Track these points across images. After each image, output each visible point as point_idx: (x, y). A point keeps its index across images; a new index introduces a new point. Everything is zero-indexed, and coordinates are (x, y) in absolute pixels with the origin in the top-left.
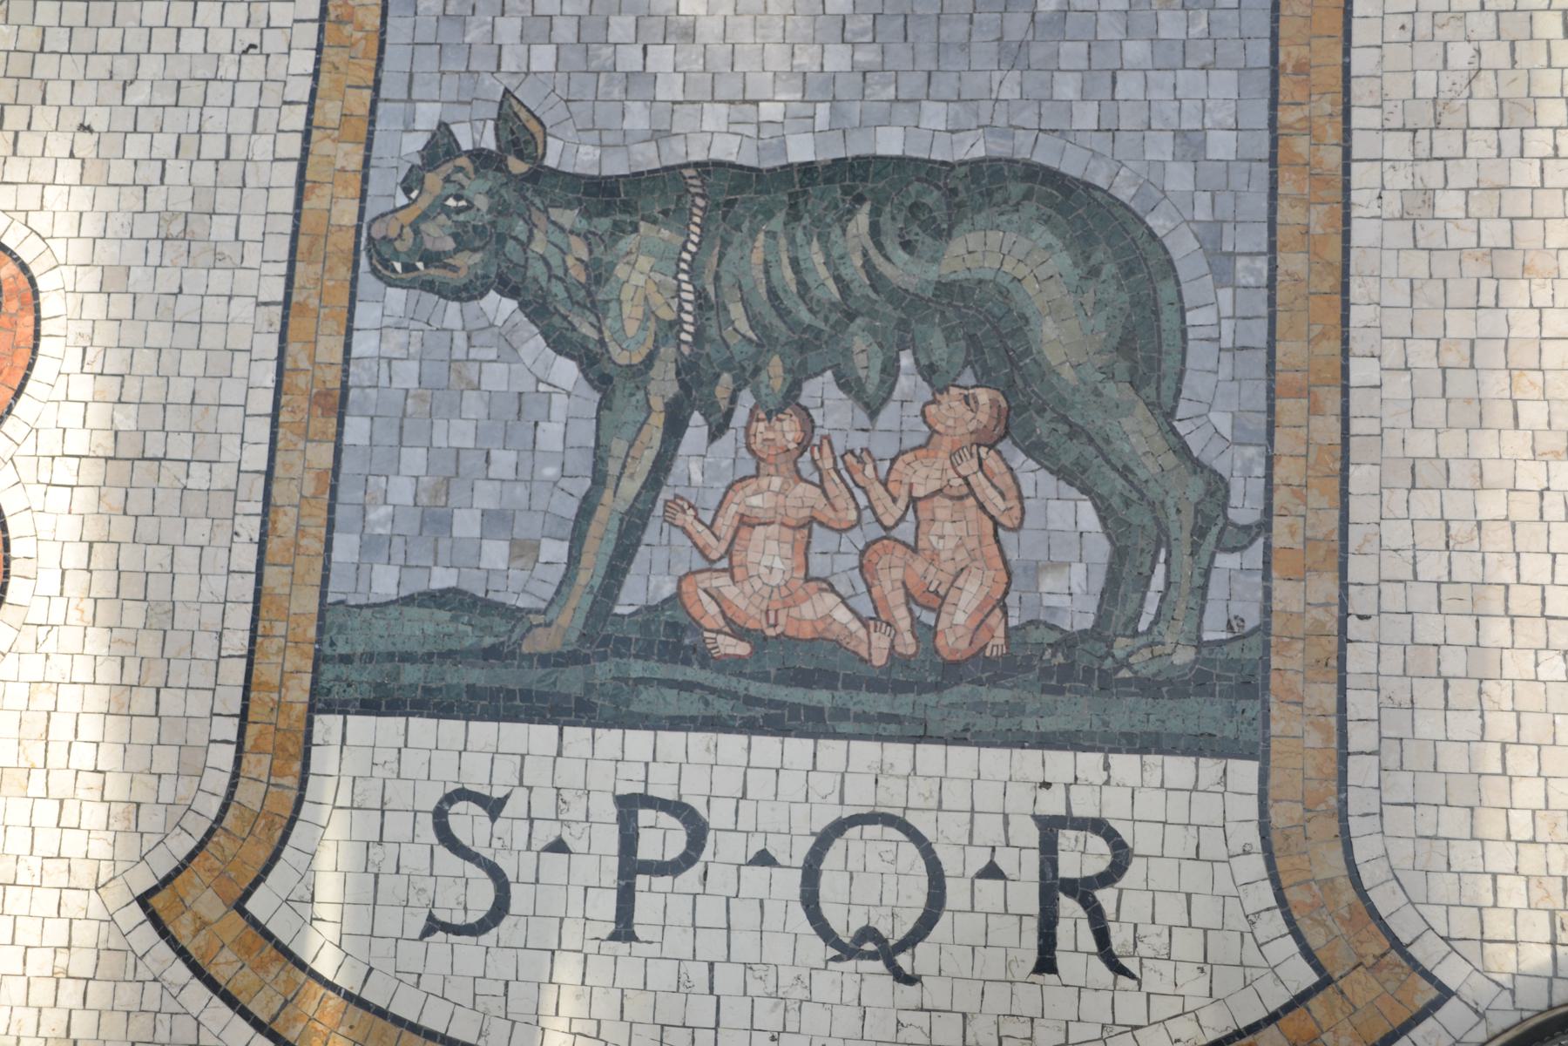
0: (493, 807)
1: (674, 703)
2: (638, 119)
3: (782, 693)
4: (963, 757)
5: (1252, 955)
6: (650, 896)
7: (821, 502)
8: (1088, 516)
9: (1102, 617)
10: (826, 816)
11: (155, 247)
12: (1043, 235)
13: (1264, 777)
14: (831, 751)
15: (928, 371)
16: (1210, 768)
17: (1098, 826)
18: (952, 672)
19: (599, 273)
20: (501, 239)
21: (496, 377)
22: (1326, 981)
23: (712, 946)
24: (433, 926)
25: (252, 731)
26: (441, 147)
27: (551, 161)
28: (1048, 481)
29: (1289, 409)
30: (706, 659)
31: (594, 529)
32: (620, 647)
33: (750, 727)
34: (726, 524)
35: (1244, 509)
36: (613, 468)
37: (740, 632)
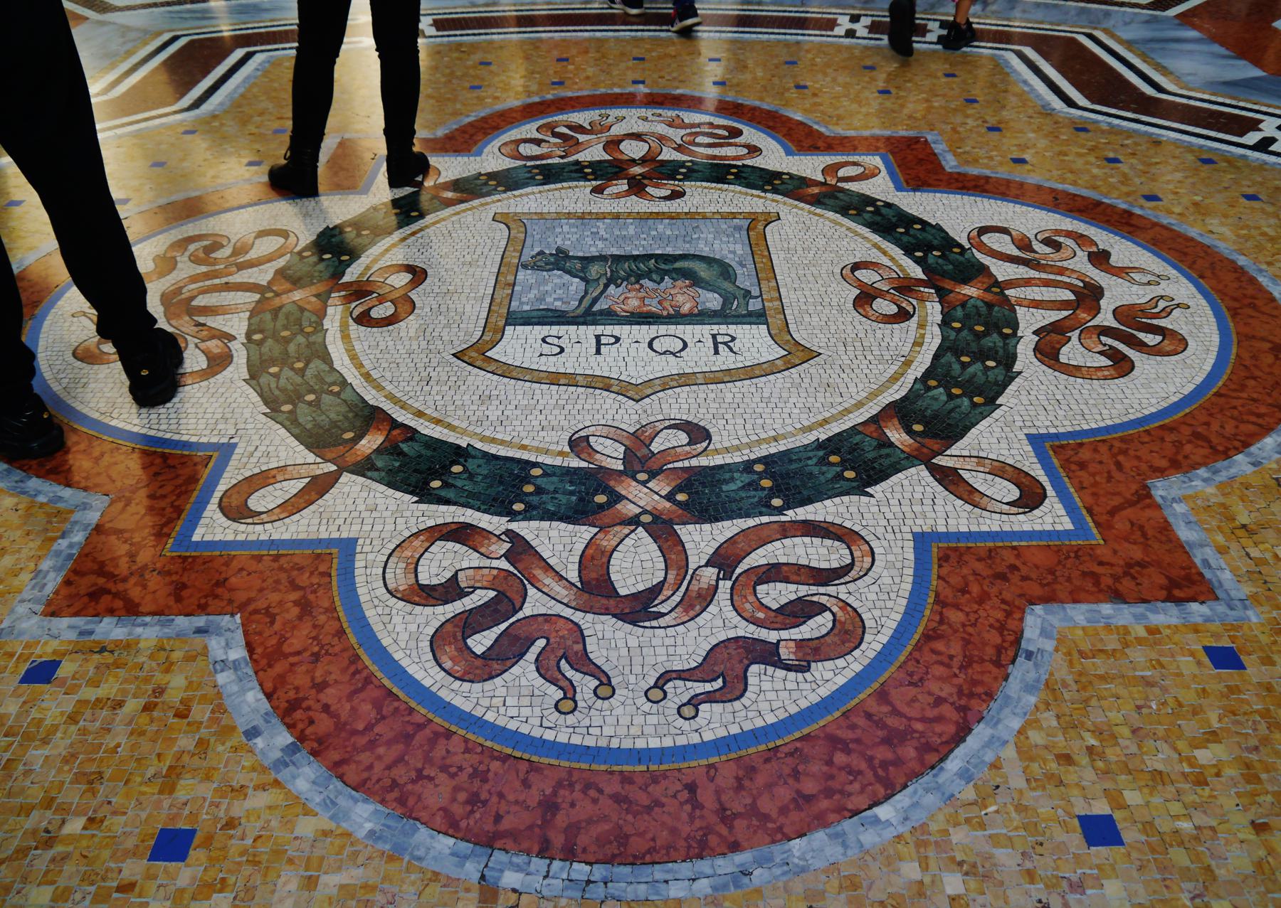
4: (690, 327)
8: (716, 295)
16: (754, 327)
18: (685, 315)
21: (557, 281)
26: (541, 253)
35: (755, 292)
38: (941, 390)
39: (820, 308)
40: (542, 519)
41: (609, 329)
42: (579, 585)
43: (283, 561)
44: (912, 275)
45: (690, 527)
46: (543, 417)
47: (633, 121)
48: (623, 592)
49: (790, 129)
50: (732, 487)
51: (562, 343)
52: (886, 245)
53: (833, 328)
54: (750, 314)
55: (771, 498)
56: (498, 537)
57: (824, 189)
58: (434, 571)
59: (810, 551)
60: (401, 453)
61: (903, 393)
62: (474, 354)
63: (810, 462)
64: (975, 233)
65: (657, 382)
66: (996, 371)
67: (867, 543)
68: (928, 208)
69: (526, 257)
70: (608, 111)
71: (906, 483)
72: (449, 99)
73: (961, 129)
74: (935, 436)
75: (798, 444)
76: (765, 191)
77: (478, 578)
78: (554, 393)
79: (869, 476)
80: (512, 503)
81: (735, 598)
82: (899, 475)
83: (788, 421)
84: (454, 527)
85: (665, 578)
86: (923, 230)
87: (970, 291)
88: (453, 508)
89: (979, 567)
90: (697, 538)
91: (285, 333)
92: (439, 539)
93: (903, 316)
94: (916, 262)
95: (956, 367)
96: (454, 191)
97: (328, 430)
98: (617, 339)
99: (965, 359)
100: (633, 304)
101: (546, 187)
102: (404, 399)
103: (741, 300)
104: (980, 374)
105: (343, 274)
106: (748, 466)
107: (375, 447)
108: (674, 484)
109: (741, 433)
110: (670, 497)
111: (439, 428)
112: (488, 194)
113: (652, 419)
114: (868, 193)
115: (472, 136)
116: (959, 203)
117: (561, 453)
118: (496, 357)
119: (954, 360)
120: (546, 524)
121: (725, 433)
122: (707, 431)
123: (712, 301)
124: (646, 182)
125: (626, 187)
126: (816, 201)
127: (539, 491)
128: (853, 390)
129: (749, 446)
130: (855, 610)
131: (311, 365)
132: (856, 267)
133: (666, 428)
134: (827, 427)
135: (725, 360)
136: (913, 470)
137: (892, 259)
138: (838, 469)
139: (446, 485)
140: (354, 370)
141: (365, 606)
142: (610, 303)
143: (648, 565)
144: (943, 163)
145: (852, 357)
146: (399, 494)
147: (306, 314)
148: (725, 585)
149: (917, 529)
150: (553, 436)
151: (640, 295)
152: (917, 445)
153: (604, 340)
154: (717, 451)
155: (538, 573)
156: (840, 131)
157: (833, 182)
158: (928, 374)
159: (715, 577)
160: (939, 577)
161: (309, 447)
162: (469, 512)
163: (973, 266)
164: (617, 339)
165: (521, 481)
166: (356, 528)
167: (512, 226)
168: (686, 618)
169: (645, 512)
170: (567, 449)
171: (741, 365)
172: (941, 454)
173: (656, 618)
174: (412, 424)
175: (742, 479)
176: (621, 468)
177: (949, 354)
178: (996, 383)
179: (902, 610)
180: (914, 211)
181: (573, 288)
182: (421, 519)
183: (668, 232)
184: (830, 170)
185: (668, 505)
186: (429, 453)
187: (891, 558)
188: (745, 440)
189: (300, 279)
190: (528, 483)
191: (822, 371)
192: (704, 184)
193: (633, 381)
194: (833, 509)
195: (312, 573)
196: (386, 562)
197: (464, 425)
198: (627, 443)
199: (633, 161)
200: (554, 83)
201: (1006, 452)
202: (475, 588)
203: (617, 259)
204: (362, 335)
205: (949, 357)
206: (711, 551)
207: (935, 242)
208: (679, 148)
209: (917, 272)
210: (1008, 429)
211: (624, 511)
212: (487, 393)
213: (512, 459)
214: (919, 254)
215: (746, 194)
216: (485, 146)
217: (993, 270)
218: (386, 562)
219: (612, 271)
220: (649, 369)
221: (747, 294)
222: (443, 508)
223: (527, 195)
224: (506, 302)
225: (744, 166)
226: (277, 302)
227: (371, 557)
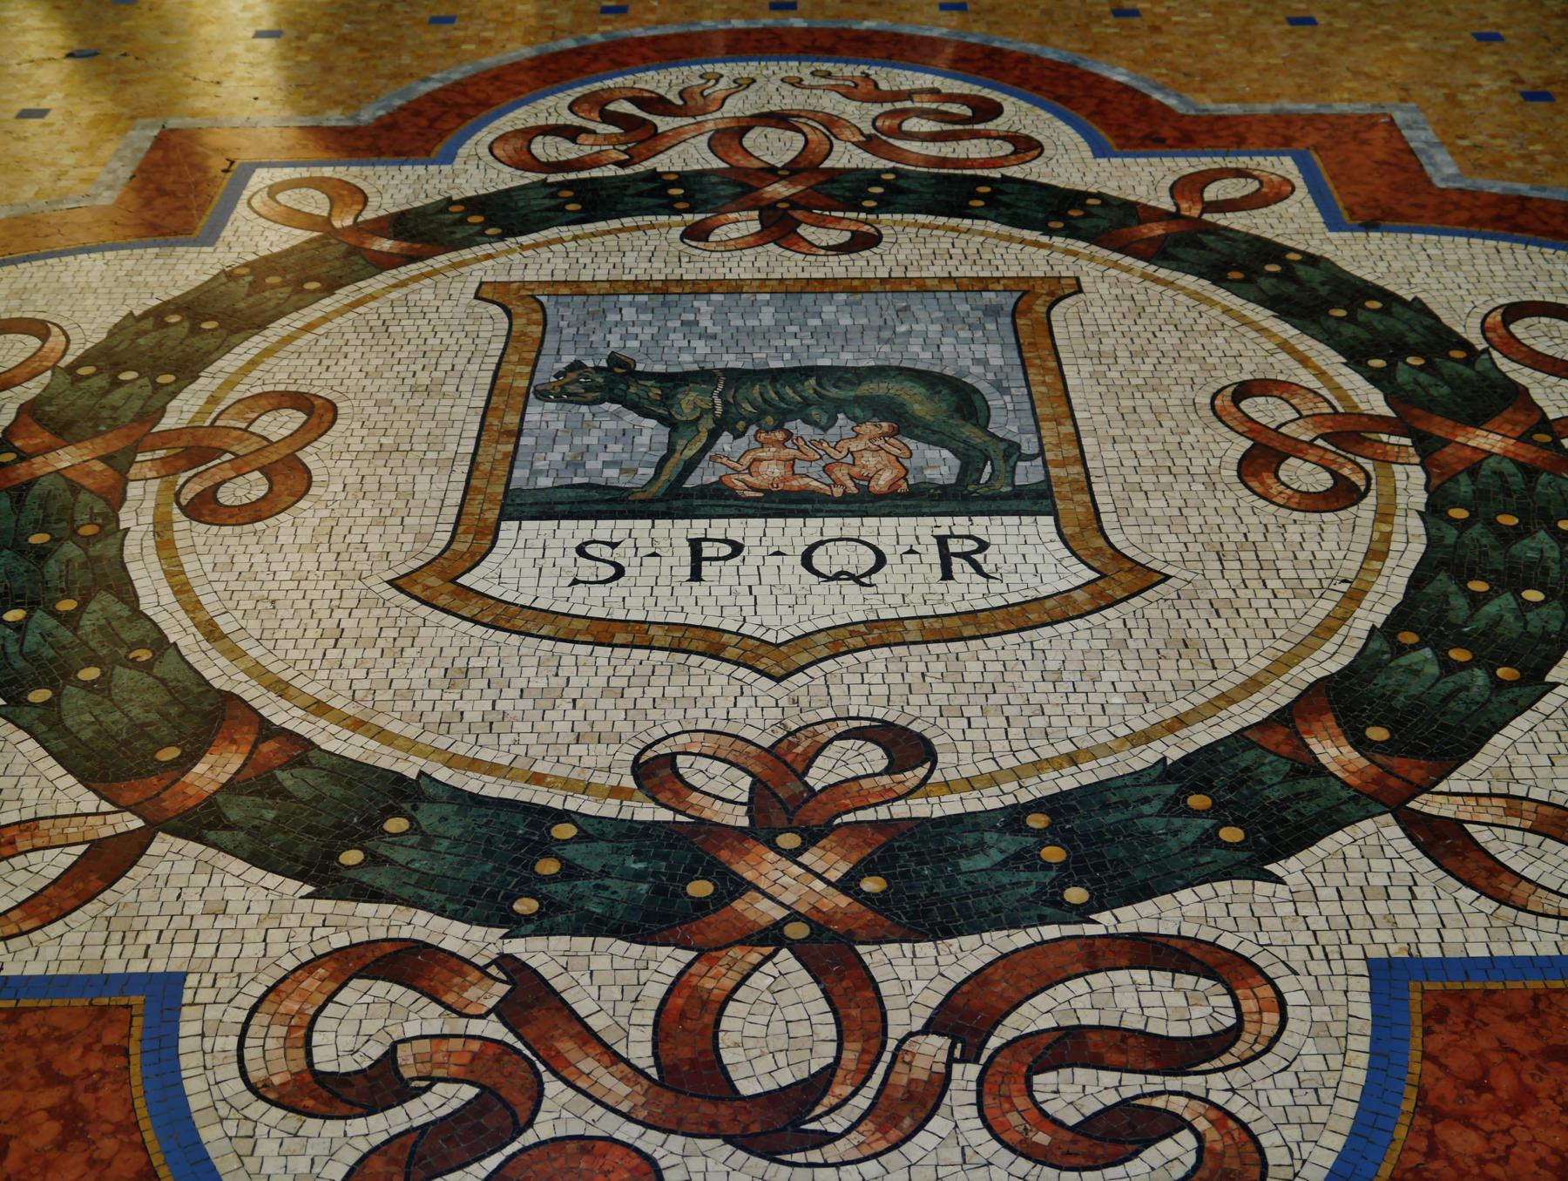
0: (614, 545)
1: (720, 510)
6: (707, 569)
7: (798, 454)
8: (946, 453)
10: (818, 538)
11: (408, 395)
14: (817, 522)
15: (854, 419)
16: (1026, 520)
18: (880, 497)
20: (611, 390)
21: (610, 425)
22: (1103, 576)
24: (575, 582)
25: (461, 529)
26: (576, 366)
27: (639, 367)
28: (922, 446)
30: (737, 498)
31: (669, 465)
33: (766, 516)
34: (746, 461)
35: (1029, 445)
36: (679, 448)
38: (1427, 652)
40: (576, 932)
41: (718, 528)
42: (653, 1072)
43: (26, 1021)
44: (1364, 407)
45: (892, 949)
46: (578, 714)
47: (771, 88)
48: (747, 1088)
49: (1103, 101)
50: (981, 862)
51: (623, 555)
52: (1306, 344)
53: (1195, 522)
54: (1019, 493)
55: (1064, 886)
56: (483, 970)
57: (1174, 227)
58: (346, 1042)
59: (1147, 999)
60: (281, 793)
61: (1344, 659)
62: (433, 581)
63: (1146, 809)
64: (1497, 317)
65: (822, 639)
66: (1544, 610)
67: (1270, 981)
68: (1396, 266)
69: (544, 376)
70: (719, 68)
71: (1352, 852)
72: (385, 45)
73: (1467, 98)
74: (1415, 752)
76: (1050, 233)
77: (439, 1058)
78: (602, 662)
79: (1273, 838)
80: (512, 898)
81: (988, 1100)
82: (1339, 835)
83: (1100, 721)
84: (388, 948)
85: (838, 1059)
86: (1385, 311)
87: (1487, 440)
88: (386, 909)
89: (1513, 1033)
90: (906, 972)
91: (38, 539)
92: (359, 975)
93: (1343, 495)
94: (1371, 380)
95: (1459, 603)
96: (395, 236)
97: (126, 743)
98: (737, 548)
99: (1478, 586)
100: (771, 472)
101: (589, 227)
102: (286, 676)
103: (1000, 463)
104: (1509, 617)
105: (162, 412)
106: (1014, 817)
107: (224, 778)
108: (855, 857)
109: (1000, 746)
110: (847, 885)
111: (359, 739)
112: (468, 243)
113: (810, 717)
114: (1268, 235)
115: (433, 121)
116: (1463, 253)
117: (617, 792)
118: (481, 587)
119: (1453, 588)
120: (583, 943)
121: (965, 747)
122: (927, 743)
123: (939, 465)
124: (798, 214)
125: (755, 227)
126: (1157, 253)
127: (570, 871)
128: (1238, 653)
129: (1016, 774)
130: (1244, 1126)
131: (93, 606)
132: (1244, 390)
133: (839, 737)
134: (1184, 732)
135: (967, 591)
136: (1367, 825)
137: (1320, 374)
138: (1208, 823)
140: (181, 615)
141: (199, 1119)
142: (722, 470)
144: (1429, 169)
145: (1236, 583)
146: (273, 880)
147: (84, 497)
148: (966, 1075)
149: (1376, 952)
150: (596, 755)
151: (785, 453)
152: (1375, 770)
153: (708, 550)
154: (948, 787)
155: (567, 1047)
156: (1209, 104)
157: (1195, 213)
158: (1398, 620)
159: (943, 1057)
160: (1426, 1056)
161: (86, 780)
162: (422, 917)
163: (1493, 387)
164: (737, 548)
165: (532, 851)
166: (182, 950)
167: (517, 309)
168: (883, 1145)
169: (794, 916)
170: (629, 782)
171: (998, 602)
172: (1427, 790)
173: (818, 1145)
174: (303, 729)
175: (1006, 845)
176: (744, 822)
177: (1442, 576)
178: (1545, 637)
179: (1346, 1126)
180: (1366, 272)
181: (643, 440)
182: (319, 932)
183: (846, 321)
184: (1187, 186)
185: (843, 901)
186: (338, 792)
187: (1321, 1013)
188: (1008, 762)
189: (71, 423)
190: (547, 854)
191: (1171, 614)
192: (921, 218)
193: (769, 637)
194: (1195, 910)
195: (88, 1049)
196: (246, 1025)
197: (412, 731)
198: (757, 769)
199: (772, 170)
200: (605, 10)
202: (434, 1081)
203: (736, 377)
204: (199, 541)
205: (1443, 582)
206: (935, 1001)
207: (1412, 338)
208: (869, 144)
209: (1374, 402)
211: (751, 915)
212: (461, 663)
213: (512, 804)
214: (1377, 363)
215: (1010, 239)
216: (460, 144)
217: (1537, 395)
218: (246, 1025)
219: (725, 404)
221: (1012, 451)
222: (366, 909)
223: (548, 243)
224: (502, 470)
225: (1005, 179)
226: (23, 471)
227: (213, 1013)
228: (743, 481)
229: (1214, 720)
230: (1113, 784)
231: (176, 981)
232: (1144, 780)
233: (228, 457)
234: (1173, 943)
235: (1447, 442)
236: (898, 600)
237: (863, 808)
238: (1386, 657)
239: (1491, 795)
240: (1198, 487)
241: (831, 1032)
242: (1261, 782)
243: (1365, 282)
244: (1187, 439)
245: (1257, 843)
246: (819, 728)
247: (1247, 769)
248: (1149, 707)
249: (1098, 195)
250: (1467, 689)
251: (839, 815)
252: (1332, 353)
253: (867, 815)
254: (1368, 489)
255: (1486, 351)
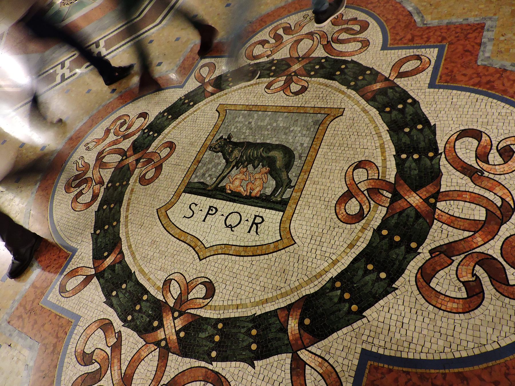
0: (196, 205)
1: (221, 197)
2: (243, 137)
3: (232, 197)
5: (274, 235)
9: (271, 194)
12: (281, 152)
13: (283, 214)
16: (277, 212)
17: (262, 217)
19: (232, 152)
23: (213, 224)
24: (185, 217)
26: (222, 137)
28: (271, 178)
29: (302, 174)
30: (225, 192)
32: (217, 190)
33: (227, 201)
37: (230, 190)
39: (318, 202)
46: (164, 261)
58: (91, 346)
71: (275, 364)
75: (245, 315)
108: (184, 324)
109: (227, 297)
124: (294, 78)
137: (384, 160)
139: (117, 295)
143: (148, 375)
145: (310, 249)
152: (298, 335)
155: (116, 361)
172: (305, 348)
176: (172, 305)
185: (175, 337)
188: (225, 303)
190: (140, 304)
191: (288, 258)
198: (182, 289)
201: (340, 360)
203: (250, 145)
210: (354, 340)
211: (159, 335)
213: (141, 285)
220: (217, 237)
225: (352, 61)
228: (229, 186)
229: (274, 303)
230: (241, 319)
231: (80, 317)
232: (248, 320)
233: (153, 162)
234: (223, 379)
235: (401, 197)
236: (235, 238)
237: (193, 309)
238: (328, 291)
239: (319, 356)
240: (323, 207)
241: (152, 377)
242: (270, 330)
243: (424, 115)
244: (333, 185)
245: (257, 352)
246: (199, 279)
247: (270, 324)
248: (263, 293)
249: (371, 69)
250: (340, 311)
251: (188, 310)
252: (394, 150)
253: (192, 311)
254: (366, 216)
255: (441, 154)
